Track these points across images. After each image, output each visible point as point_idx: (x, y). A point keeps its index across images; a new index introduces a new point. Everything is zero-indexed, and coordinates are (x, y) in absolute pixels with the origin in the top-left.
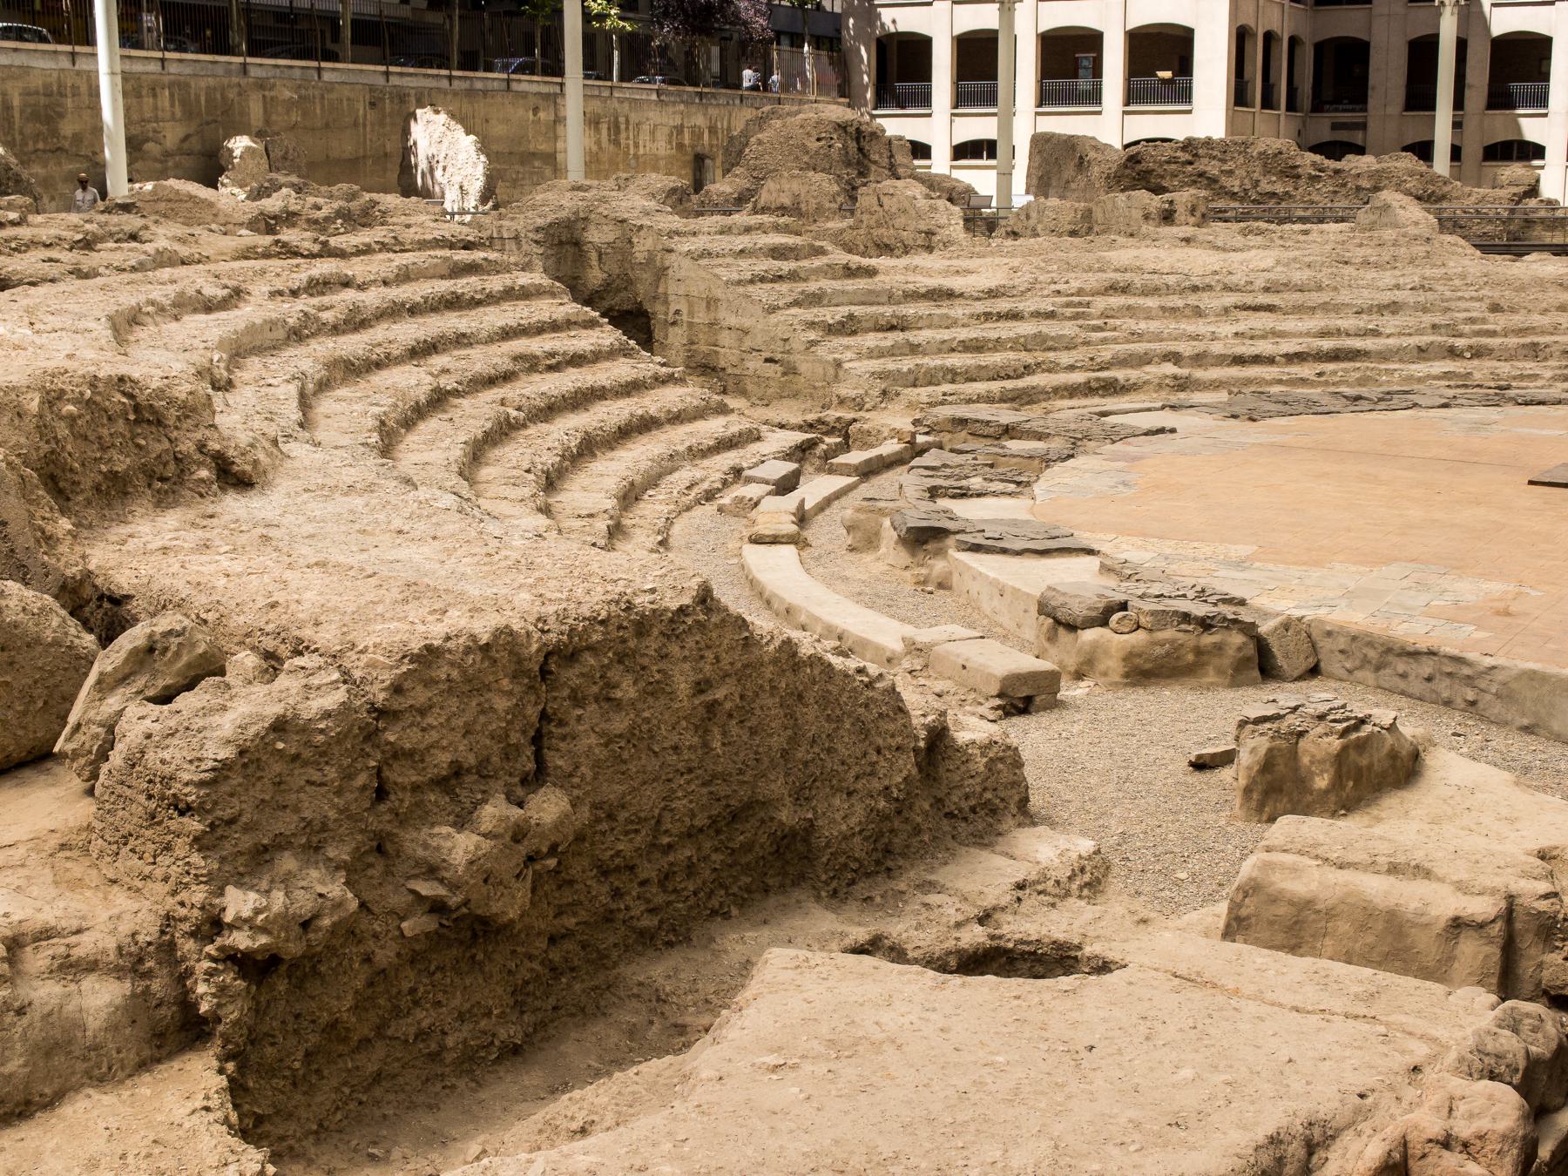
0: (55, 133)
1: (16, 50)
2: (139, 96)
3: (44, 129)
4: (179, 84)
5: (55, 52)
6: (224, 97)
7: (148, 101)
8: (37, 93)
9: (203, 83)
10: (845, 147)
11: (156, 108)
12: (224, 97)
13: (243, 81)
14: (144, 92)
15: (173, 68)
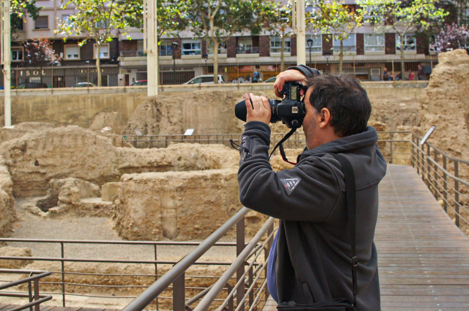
0: (44, 114)
1: (31, 91)
2: (78, 101)
3: (40, 113)
4: (95, 98)
5: (45, 91)
6: (114, 99)
7: (82, 103)
8: (38, 103)
9: (105, 96)
10: (152, 110)
11: (85, 105)
12: (114, 99)
13: (124, 94)
14: (80, 100)
15: (92, 92)
